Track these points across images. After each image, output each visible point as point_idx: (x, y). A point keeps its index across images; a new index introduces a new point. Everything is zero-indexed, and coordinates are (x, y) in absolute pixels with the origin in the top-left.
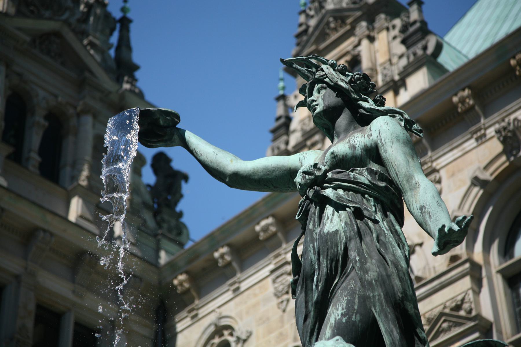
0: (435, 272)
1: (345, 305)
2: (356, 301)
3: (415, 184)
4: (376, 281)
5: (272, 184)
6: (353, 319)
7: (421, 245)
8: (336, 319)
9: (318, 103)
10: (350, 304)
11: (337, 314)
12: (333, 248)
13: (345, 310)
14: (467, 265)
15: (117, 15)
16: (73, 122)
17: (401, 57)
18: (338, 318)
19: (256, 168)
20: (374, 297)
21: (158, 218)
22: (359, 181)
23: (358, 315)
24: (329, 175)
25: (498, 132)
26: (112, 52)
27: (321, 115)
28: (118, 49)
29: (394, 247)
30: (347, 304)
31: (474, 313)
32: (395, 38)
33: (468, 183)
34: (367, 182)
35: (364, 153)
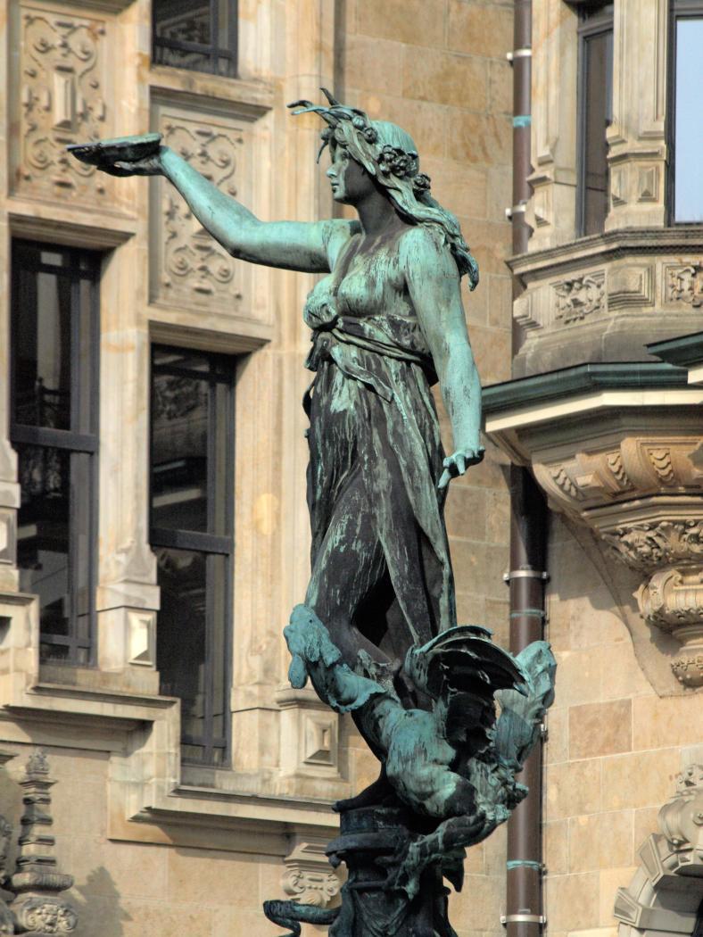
1: (345, 527)
2: (359, 521)
4: (385, 493)
6: (353, 548)
10: (351, 524)
13: (344, 536)
20: (381, 515)
23: (360, 542)
24: (341, 324)
29: (413, 440)
34: (386, 341)
35: (388, 288)
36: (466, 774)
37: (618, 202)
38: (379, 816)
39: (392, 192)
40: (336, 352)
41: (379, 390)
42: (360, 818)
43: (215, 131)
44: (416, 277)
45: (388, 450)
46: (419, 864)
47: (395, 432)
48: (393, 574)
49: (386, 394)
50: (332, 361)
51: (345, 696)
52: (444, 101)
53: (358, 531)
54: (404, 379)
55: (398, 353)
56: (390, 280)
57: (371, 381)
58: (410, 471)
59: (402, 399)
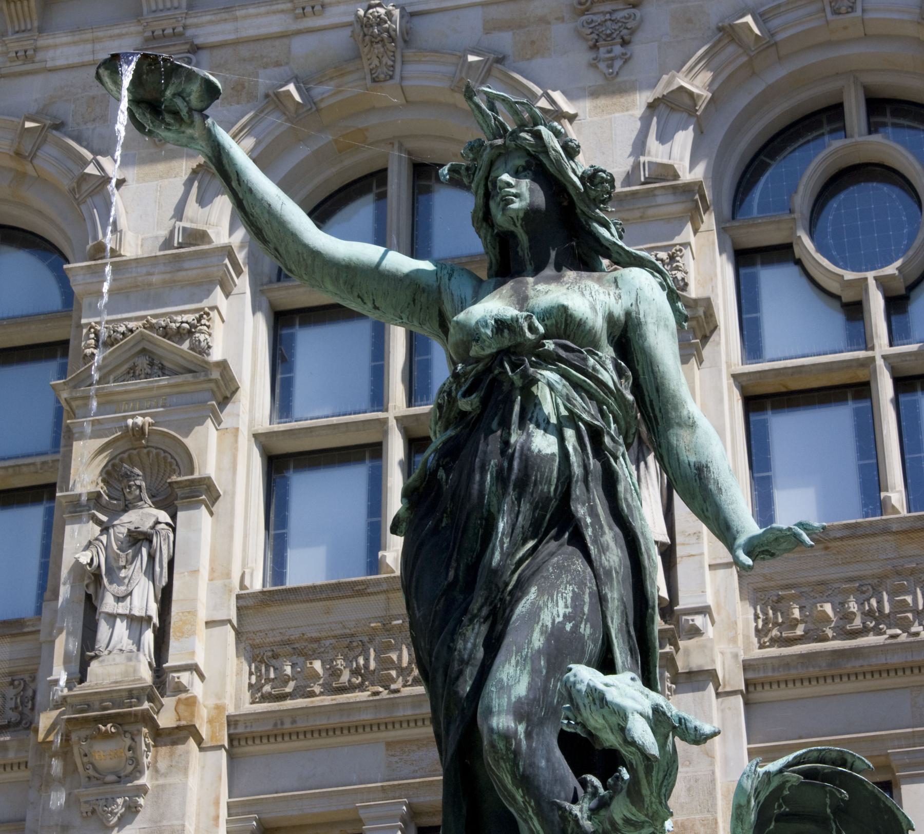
3: (687, 418)
4: (617, 573)
5: (374, 300)
8: (554, 620)
9: (519, 191)
11: (555, 613)
12: (541, 484)
13: (570, 610)
18: (558, 620)
19: (354, 258)
22: (600, 376)
23: (588, 626)
27: (517, 217)
30: (572, 598)
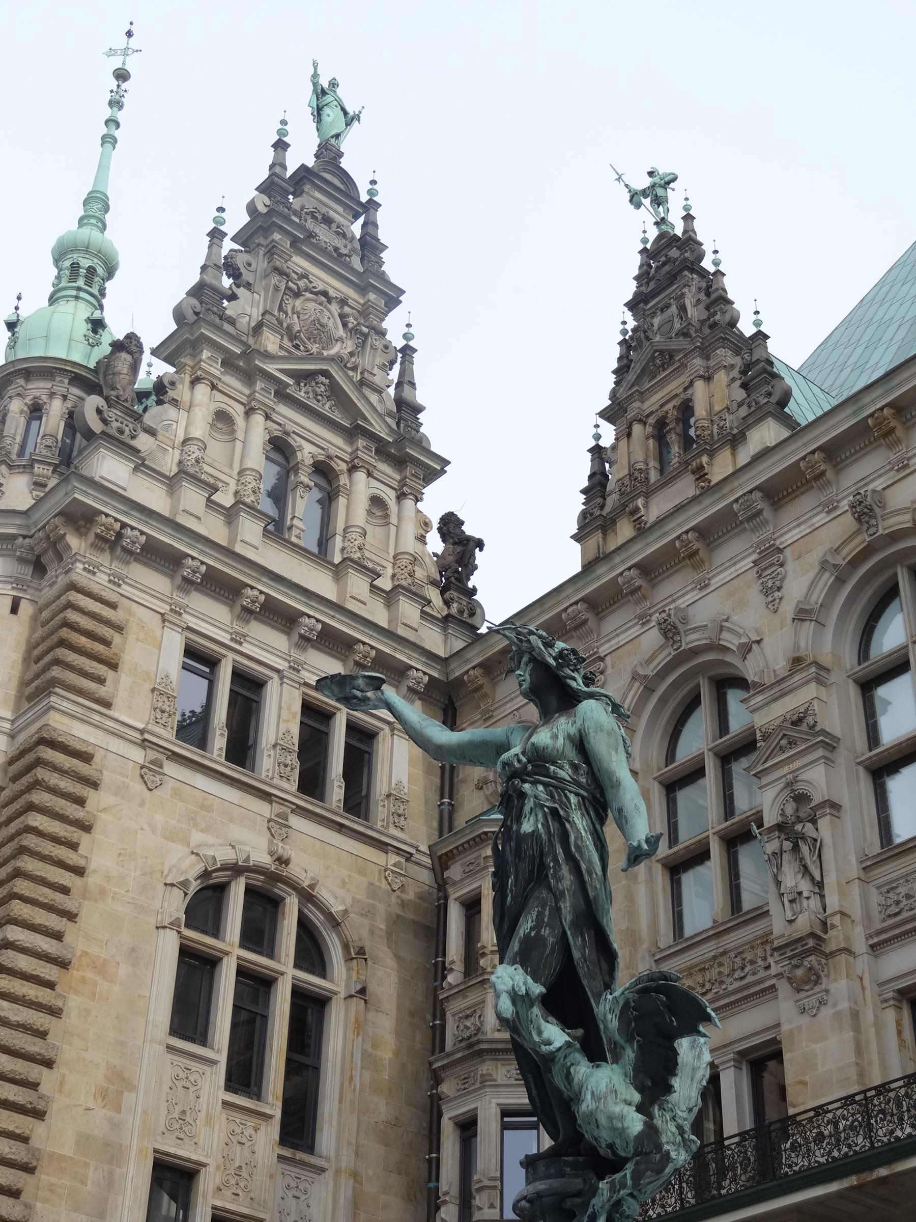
0: (775, 676)
2: (547, 912)
7: (758, 642)
10: (540, 914)
14: (813, 669)
15: (399, 343)
16: (344, 480)
17: (740, 405)
21: (447, 595)
24: (530, 767)
25: (853, 506)
26: (392, 391)
28: (399, 385)
31: (818, 728)
32: (733, 380)
33: (817, 568)
35: (567, 742)
36: (649, 1115)
37: (479, 1209)
38: (567, 1163)
39: (569, 682)
40: (527, 787)
41: (562, 813)
42: (547, 1167)
43: (303, 1178)
44: (591, 731)
45: (570, 857)
46: (609, 1200)
47: (576, 845)
48: (576, 955)
49: (568, 815)
50: (522, 795)
51: (545, 1035)
52: (400, 1174)
53: (546, 920)
54: (580, 809)
55: (574, 788)
56: (569, 735)
57: (557, 806)
58: (590, 874)
59: (580, 822)
